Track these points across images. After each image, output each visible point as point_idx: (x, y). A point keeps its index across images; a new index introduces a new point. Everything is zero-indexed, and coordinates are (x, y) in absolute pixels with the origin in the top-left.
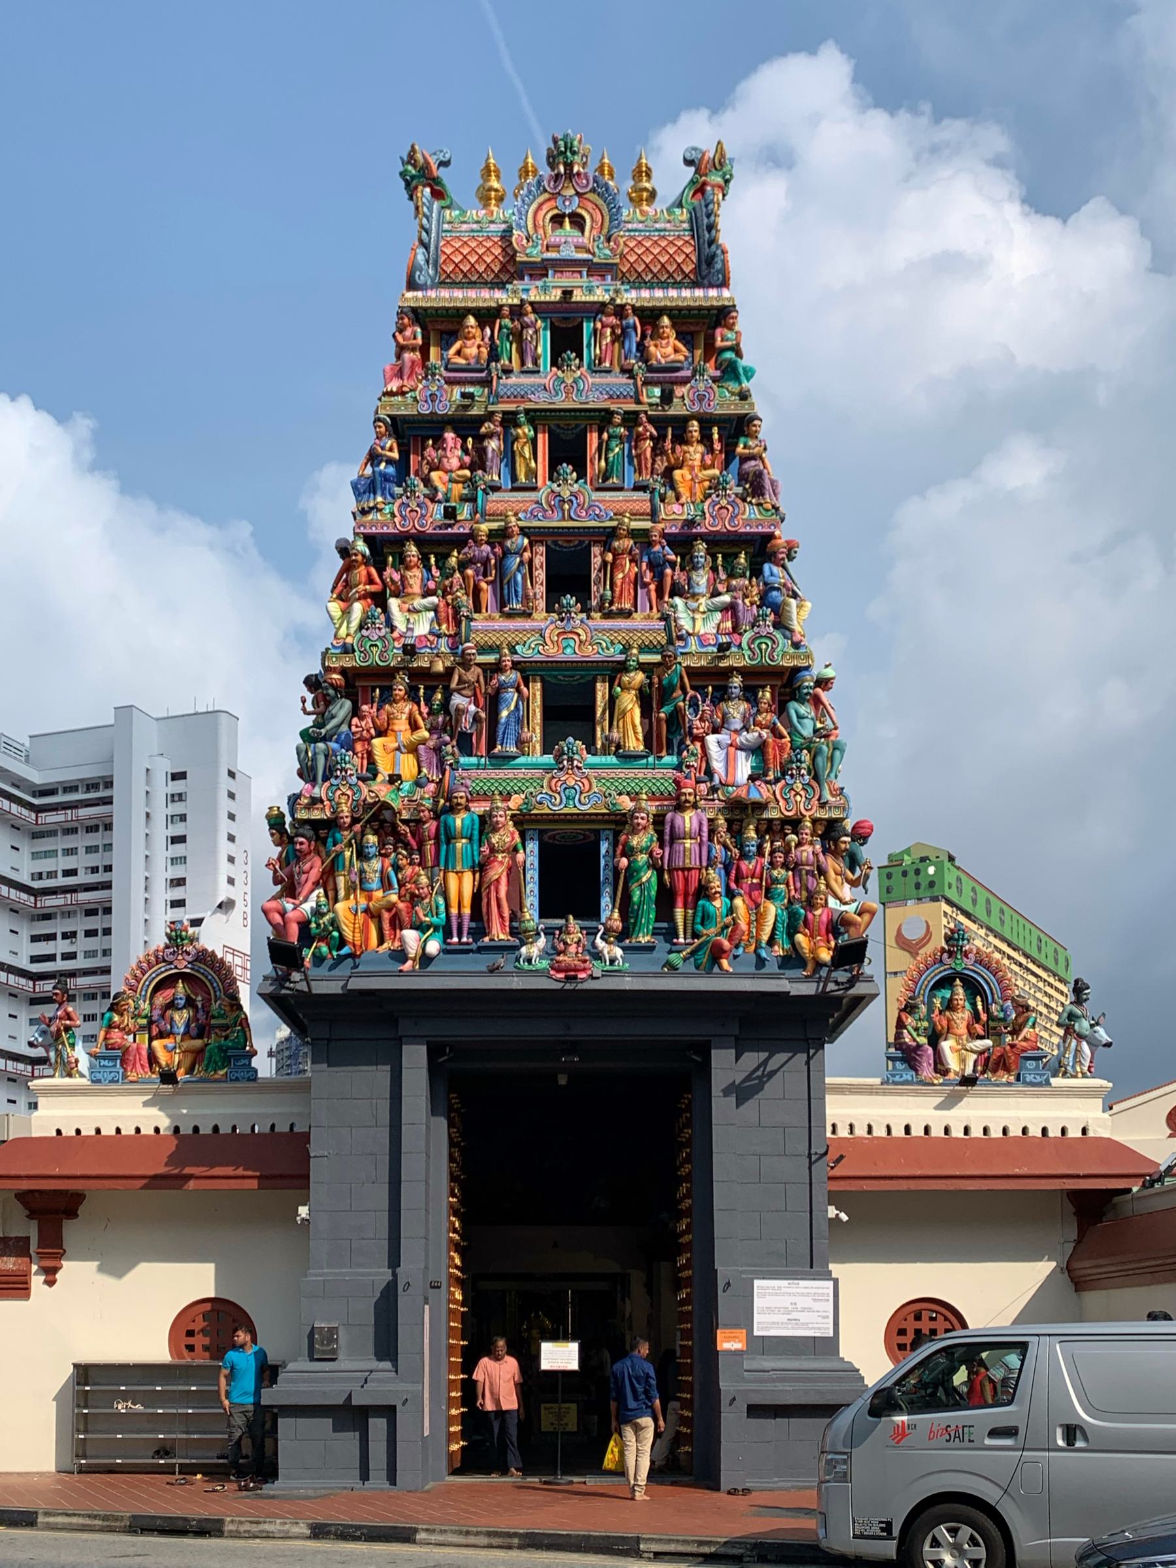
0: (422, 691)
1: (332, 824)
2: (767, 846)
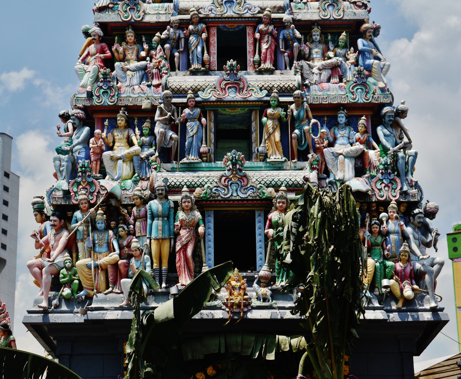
0: (136, 121)
1: (76, 207)
2: (368, 220)
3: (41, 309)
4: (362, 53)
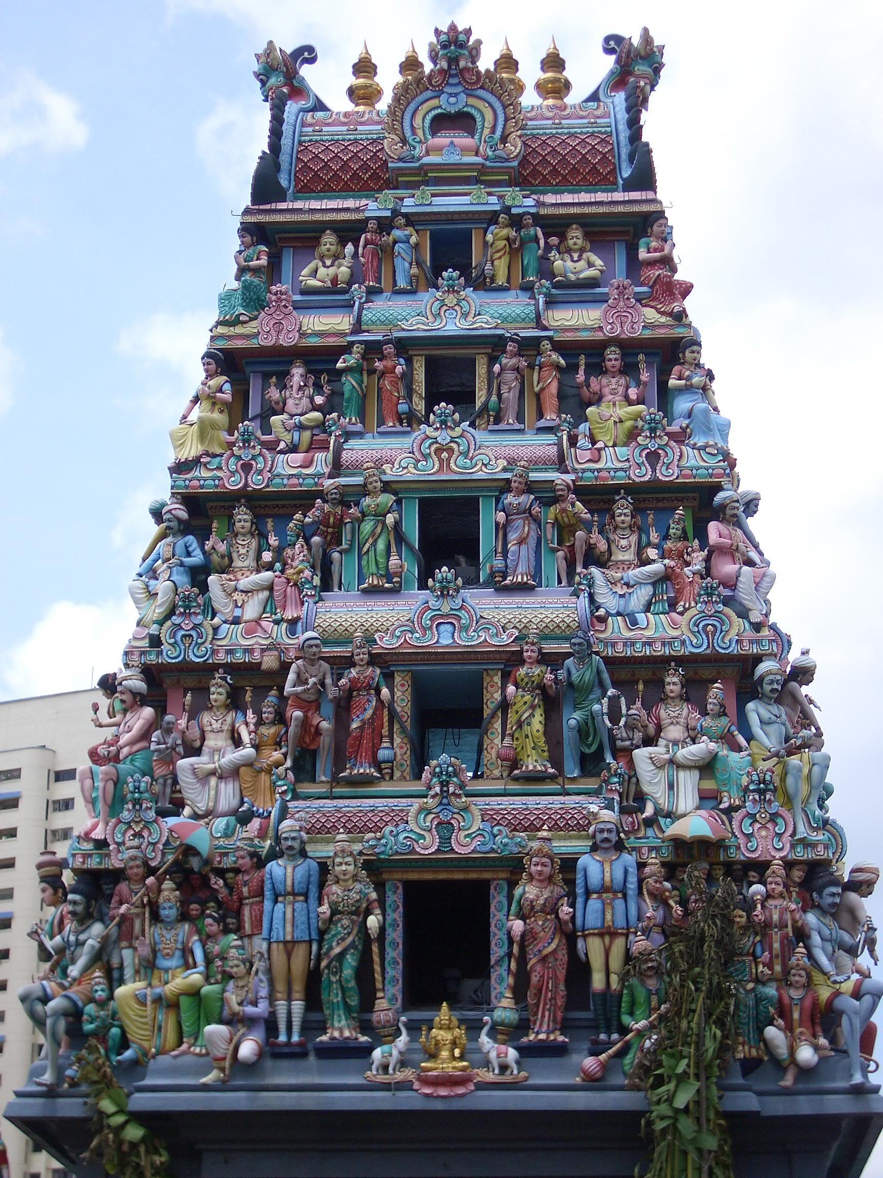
0: (249, 694)
1: (117, 875)
3: (44, 1088)
4: (712, 552)
